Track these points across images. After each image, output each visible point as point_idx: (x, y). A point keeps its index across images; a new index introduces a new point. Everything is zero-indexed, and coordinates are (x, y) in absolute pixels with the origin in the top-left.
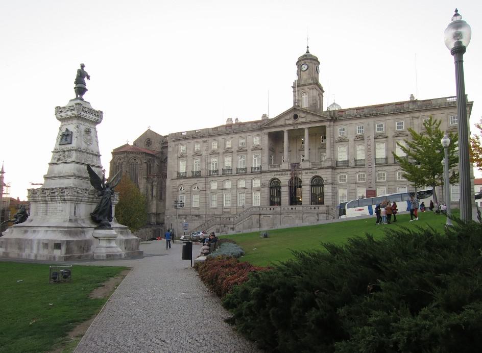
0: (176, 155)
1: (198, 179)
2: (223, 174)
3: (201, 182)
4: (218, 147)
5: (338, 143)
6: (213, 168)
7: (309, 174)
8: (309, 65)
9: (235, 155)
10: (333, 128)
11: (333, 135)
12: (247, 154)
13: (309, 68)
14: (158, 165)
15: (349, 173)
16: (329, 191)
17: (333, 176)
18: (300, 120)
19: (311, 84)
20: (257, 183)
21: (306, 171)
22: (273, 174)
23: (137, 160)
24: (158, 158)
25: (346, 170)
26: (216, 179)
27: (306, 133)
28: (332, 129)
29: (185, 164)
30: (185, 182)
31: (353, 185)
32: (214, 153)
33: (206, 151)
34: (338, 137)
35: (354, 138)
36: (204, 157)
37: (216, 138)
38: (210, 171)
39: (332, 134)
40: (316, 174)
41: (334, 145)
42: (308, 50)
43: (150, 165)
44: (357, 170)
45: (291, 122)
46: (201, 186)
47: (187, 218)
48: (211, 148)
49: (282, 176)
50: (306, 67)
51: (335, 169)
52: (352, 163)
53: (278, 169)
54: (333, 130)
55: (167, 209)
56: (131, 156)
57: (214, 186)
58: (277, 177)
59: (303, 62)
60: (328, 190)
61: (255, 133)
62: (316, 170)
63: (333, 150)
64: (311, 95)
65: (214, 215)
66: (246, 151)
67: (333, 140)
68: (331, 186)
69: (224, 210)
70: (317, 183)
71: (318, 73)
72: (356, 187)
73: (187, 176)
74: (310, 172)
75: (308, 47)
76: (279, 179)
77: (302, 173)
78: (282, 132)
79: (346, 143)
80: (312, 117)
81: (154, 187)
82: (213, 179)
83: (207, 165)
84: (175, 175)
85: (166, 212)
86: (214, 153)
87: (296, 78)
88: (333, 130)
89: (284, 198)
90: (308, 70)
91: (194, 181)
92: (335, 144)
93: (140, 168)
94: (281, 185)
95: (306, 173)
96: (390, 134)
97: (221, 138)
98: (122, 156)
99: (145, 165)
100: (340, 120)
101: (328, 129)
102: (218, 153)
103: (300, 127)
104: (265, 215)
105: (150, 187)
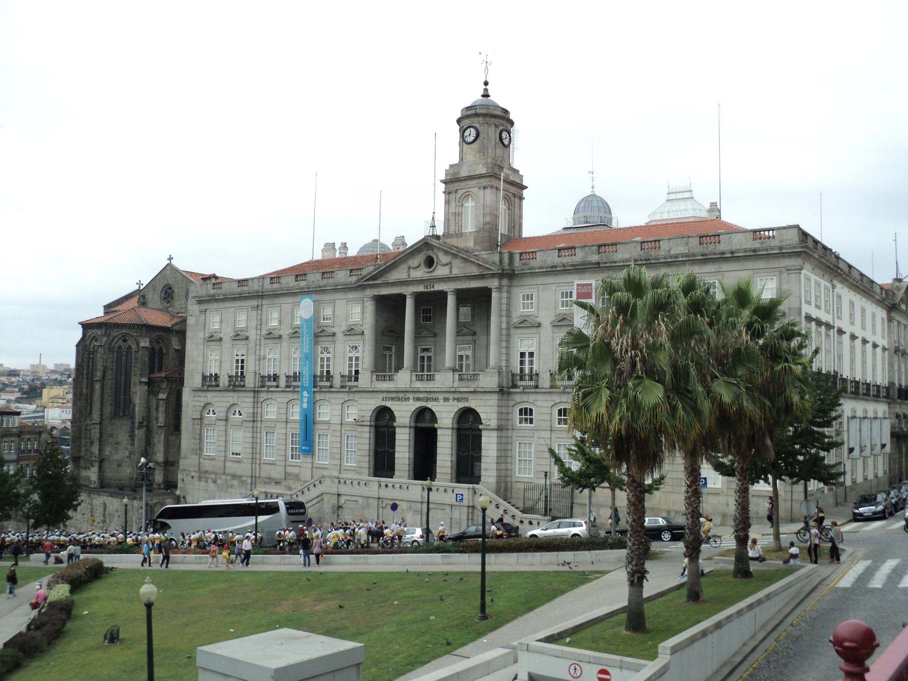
0: (201, 335)
1: (241, 394)
2: (287, 386)
3: (245, 402)
4: (280, 323)
5: (519, 331)
6: (268, 369)
7: (451, 401)
8: (480, 129)
10: (508, 292)
11: (508, 310)
13: (481, 137)
14: (177, 350)
17: (504, 410)
18: (441, 271)
19: (480, 176)
21: (447, 396)
22: (381, 396)
23: (130, 343)
24: (178, 332)
25: (532, 397)
26: (275, 395)
27: (451, 301)
28: (504, 295)
29: (217, 358)
30: (216, 399)
32: (273, 337)
33: (256, 329)
34: (519, 314)
35: (553, 319)
36: (252, 344)
37: (277, 301)
38: (263, 377)
39: (504, 307)
40: (467, 405)
41: (508, 335)
42: (486, 90)
43: (161, 349)
44: (557, 398)
45: (420, 273)
47: (219, 481)
48: (267, 323)
49: (396, 403)
50: (473, 131)
51: (509, 393)
54: (509, 298)
55: (182, 455)
56: (115, 333)
57: (271, 411)
58: (388, 404)
59: (466, 122)
60: (489, 444)
61: (351, 295)
62: (465, 396)
63: (508, 348)
64: (482, 202)
65: (269, 478)
66: (334, 334)
67: (508, 323)
68: (495, 434)
69: (289, 470)
71: (507, 147)
72: (554, 439)
73: (221, 385)
74: (454, 399)
75: (486, 83)
77: (436, 400)
78: (402, 298)
79: (534, 330)
80: (463, 265)
81: (161, 403)
82: (270, 395)
84: (198, 382)
85: (182, 462)
86: (273, 337)
87: (456, 160)
88: (509, 298)
90: (478, 141)
91: (231, 398)
92: (512, 331)
94: (395, 424)
95: (446, 400)
98: (99, 332)
99: (147, 353)
100: (523, 275)
101: (494, 295)
102: (280, 337)
103: (438, 287)
104: (349, 498)
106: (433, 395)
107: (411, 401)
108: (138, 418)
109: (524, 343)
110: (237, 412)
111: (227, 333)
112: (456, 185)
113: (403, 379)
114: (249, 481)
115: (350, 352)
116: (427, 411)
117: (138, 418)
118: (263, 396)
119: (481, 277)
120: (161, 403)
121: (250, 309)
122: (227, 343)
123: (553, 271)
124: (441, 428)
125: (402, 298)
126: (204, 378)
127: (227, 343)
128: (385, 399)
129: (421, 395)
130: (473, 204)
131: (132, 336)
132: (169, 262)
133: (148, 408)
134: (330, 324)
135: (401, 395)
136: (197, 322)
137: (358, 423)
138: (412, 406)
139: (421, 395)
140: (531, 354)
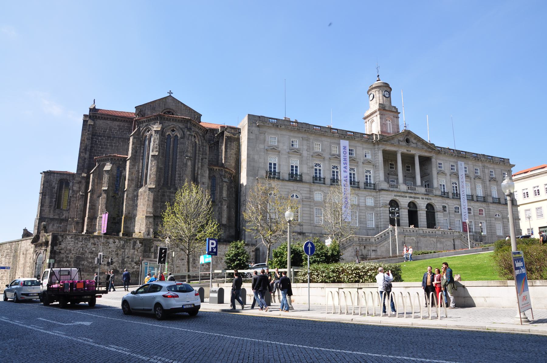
4: (322, 150)
7: (425, 199)
12: (357, 166)
15: (449, 204)
16: (442, 219)
20: (370, 202)
21: (423, 197)
22: (394, 194)
31: (453, 216)
46: (304, 195)
48: (313, 149)
53: (398, 190)
58: (397, 198)
73: (281, 178)
74: (426, 198)
76: (399, 200)
77: (418, 198)
80: (422, 146)
83: (309, 170)
89: (405, 222)
93: (199, 151)
95: (423, 198)
96: (472, 176)
97: (326, 141)
101: (433, 160)
103: (413, 152)
106: (417, 196)
107: (408, 198)
110: (295, 196)
112: (384, 112)
114: (311, 235)
115: (366, 172)
116: (411, 203)
119: (430, 152)
120: (225, 184)
121: (301, 139)
124: (422, 210)
128: (395, 196)
129: (412, 195)
130: (389, 122)
131: (200, 135)
132: (169, 95)
134: (355, 157)
135: (403, 195)
136: (257, 138)
138: (409, 200)
139: (412, 195)
140: (444, 185)
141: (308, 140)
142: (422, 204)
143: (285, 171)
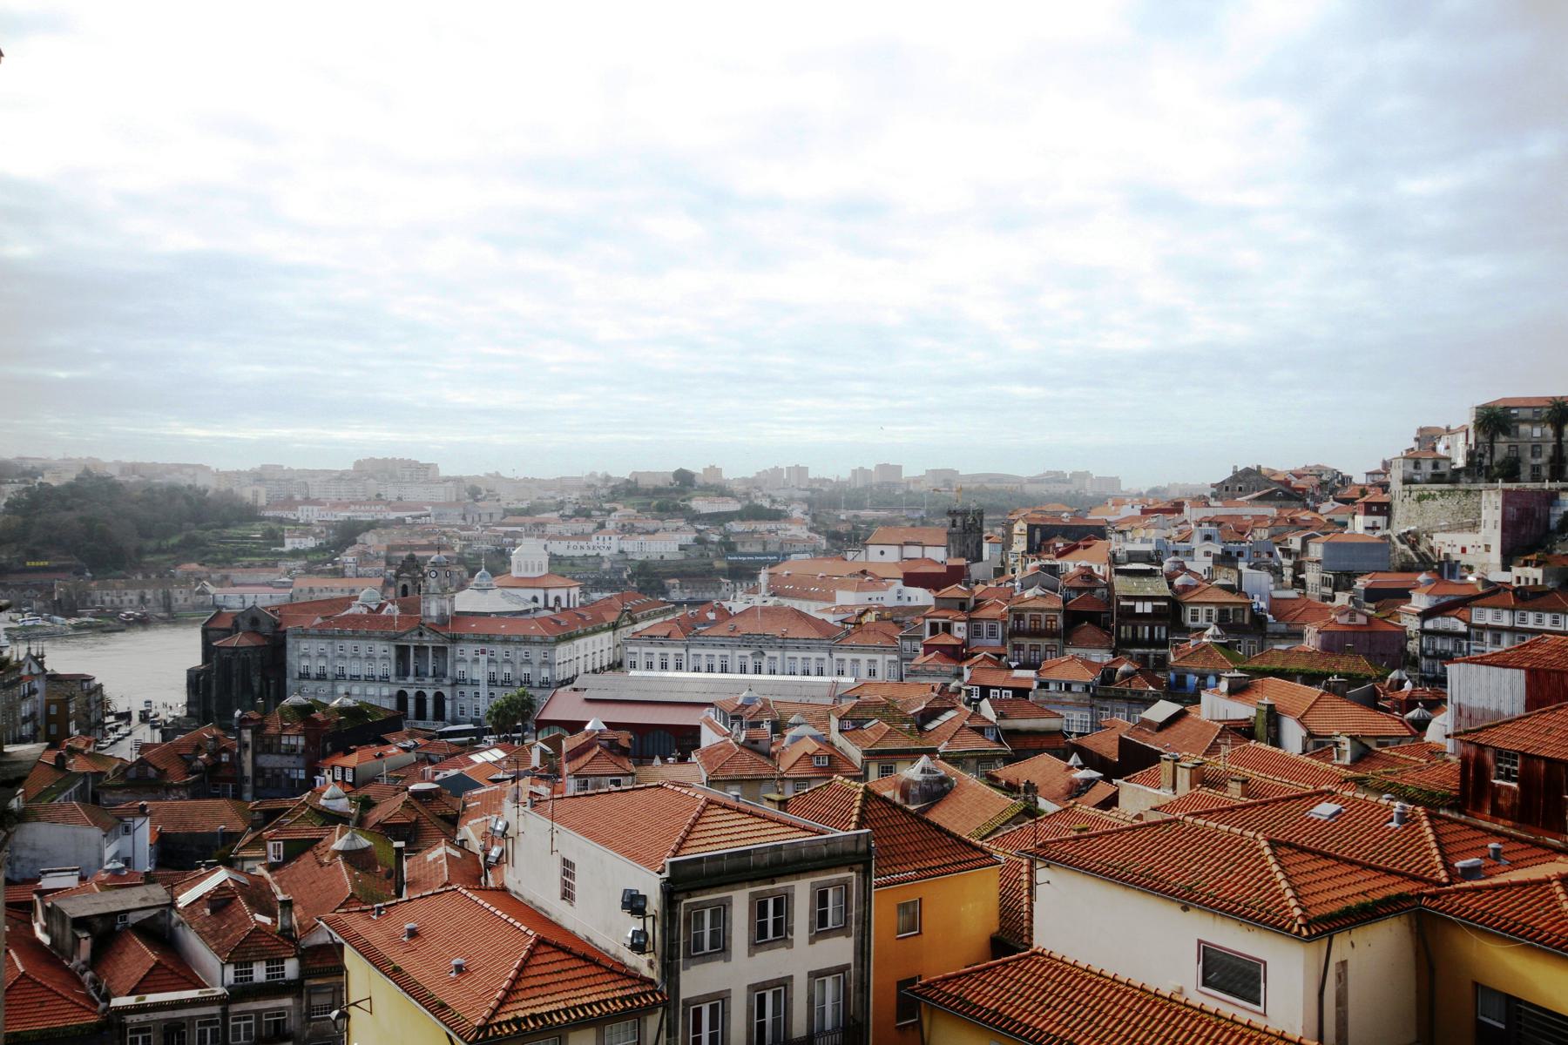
9: (363, 661)
18: (426, 638)
20: (386, 691)
25: (464, 687)
27: (430, 650)
44: (473, 688)
52: (469, 682)
60: (448, 705)
61: (383, 643)
70: (439, 698)
78: (408, 648)
84: (297, 675)
91: (318, 684)
96: (499, 660)
98: (231, 651)
105: (264, 684)
108: (256, 689)
109: (461, 667)
111: (313, 652)
113: (411, 679)
117: (256, 689)
118: (337, 683)
122: (314, 660)
123: (472, 641)
125: (408, 648)
126: (300, 674)
127: (314, 660)
133: (261, 687)
136: (293, 647)
137: (390, 696)
138: (415, 690)
141: (331, 643)
142: (430, 694)
143: (314, 671)
